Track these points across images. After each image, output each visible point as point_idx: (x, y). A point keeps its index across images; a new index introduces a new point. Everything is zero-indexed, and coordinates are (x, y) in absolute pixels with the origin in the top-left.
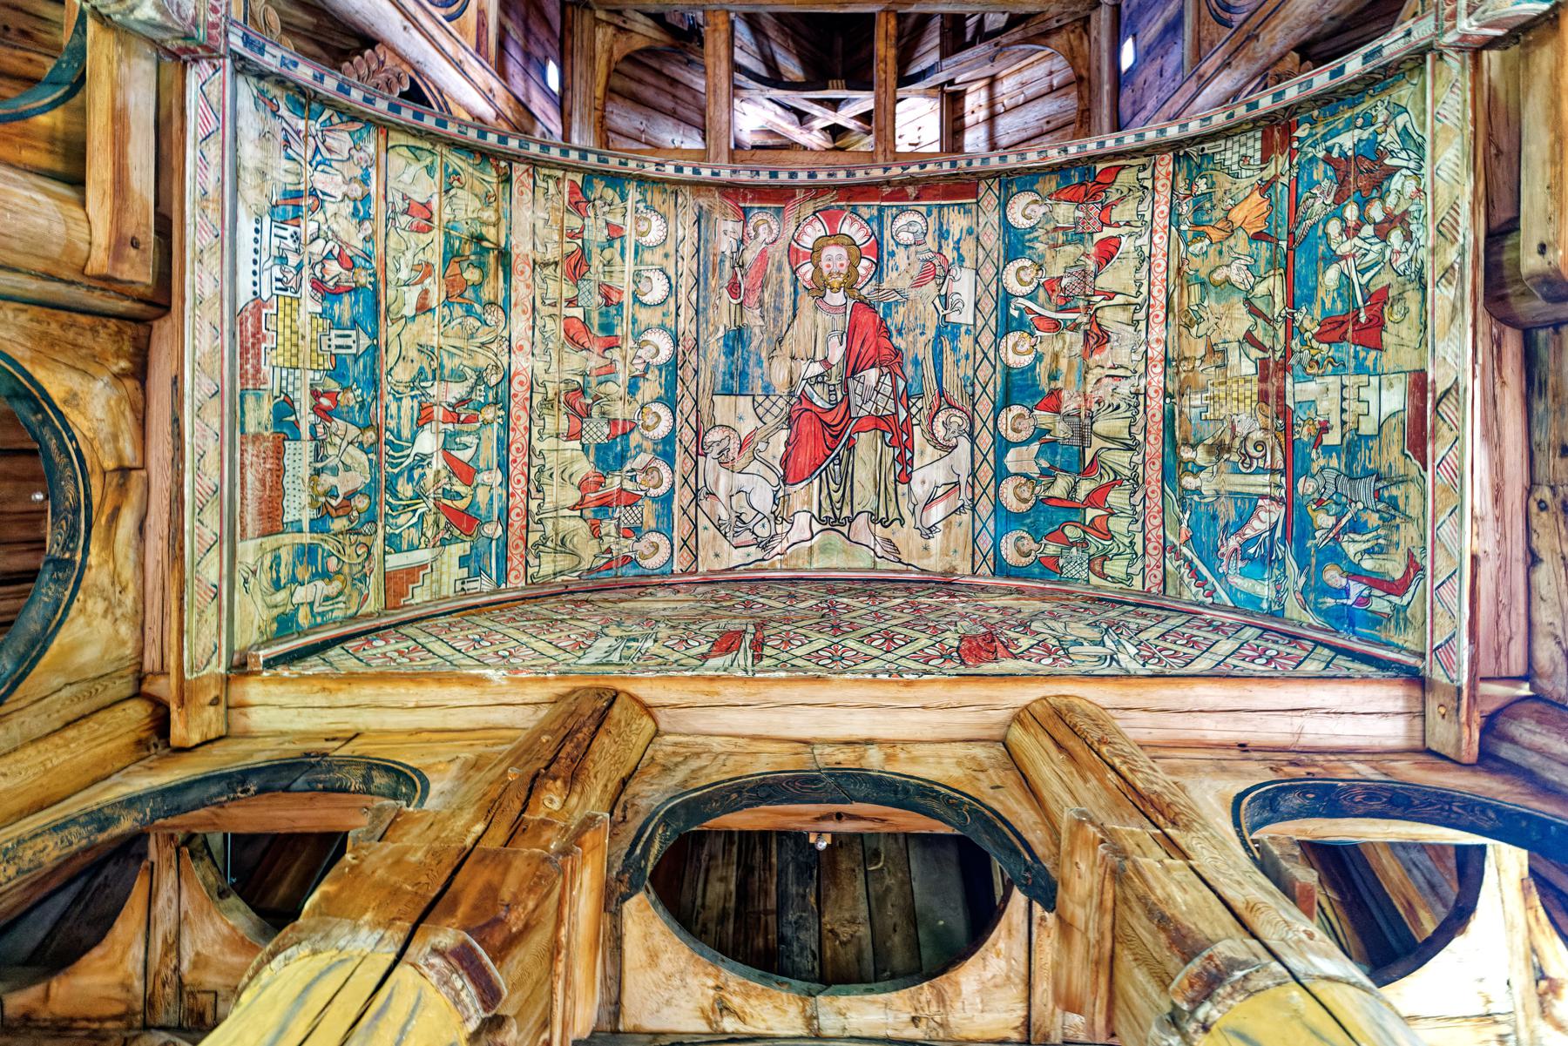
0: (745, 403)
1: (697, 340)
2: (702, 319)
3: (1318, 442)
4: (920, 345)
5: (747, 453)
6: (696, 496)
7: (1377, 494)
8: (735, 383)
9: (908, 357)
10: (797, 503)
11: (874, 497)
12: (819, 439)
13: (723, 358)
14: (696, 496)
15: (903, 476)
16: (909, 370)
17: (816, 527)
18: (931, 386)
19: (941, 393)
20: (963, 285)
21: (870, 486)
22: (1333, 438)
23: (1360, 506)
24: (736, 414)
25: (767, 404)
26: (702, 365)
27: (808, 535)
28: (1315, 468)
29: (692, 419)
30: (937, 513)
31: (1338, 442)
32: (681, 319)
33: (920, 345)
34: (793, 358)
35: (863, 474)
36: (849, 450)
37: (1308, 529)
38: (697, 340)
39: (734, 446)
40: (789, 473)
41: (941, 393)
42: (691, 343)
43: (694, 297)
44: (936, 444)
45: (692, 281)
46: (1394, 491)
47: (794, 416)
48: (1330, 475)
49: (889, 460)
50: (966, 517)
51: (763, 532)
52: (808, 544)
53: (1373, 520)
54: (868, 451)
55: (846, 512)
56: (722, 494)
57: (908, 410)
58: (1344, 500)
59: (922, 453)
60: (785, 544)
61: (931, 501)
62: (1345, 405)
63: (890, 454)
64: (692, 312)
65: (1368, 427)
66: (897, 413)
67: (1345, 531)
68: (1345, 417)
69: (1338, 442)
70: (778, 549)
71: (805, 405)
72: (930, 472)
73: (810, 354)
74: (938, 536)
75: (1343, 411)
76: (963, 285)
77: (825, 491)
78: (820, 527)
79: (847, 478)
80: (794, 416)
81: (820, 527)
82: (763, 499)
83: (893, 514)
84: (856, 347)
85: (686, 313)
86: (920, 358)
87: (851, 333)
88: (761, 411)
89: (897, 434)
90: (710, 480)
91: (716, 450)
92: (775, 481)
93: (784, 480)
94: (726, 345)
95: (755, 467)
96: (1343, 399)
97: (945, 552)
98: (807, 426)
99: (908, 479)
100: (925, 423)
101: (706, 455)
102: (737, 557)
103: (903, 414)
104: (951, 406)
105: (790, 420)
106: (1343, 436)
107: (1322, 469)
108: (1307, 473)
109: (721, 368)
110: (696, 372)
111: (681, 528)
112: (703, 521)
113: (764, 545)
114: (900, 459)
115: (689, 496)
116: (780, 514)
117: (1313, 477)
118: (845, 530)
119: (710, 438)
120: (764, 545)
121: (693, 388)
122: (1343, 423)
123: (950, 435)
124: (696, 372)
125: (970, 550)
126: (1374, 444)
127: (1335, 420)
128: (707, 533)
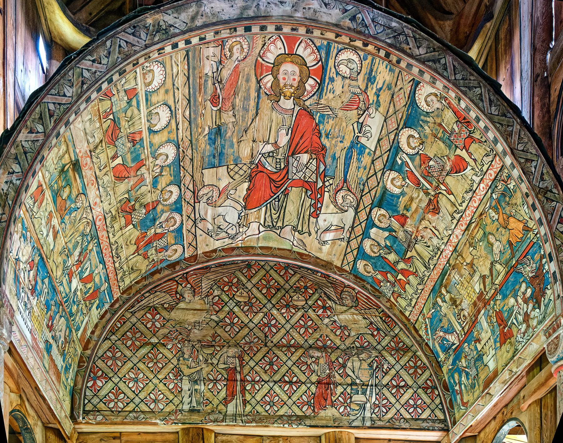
0: (222, 171)
1: (191, 141)
2: (193, 125)
4: (338, 149)
5: (223, 196)
6: (195, 222)
8: (217, 159)
9: (329, 154)
10: (252, 218)
11: (296, 220)
12: (267, 186)
13: (208, 147)
14: (195, 222)
15: (314, 214)
16: (329, 160)
17: (262, 229)
18: (340, 174)
19: (345, 181)
20: (374, 122)
21: (295, 214)
24: (219, 177)
25: (236, 169)
26: (195, 155)
27: (258, 232)
29: (191, 187)
30: (329, 236)
32: (180, 131)
33: (338, 149)
34: (254, 141)
35: (292, 208)
36: (285, 195)
38: (191, 141)
39: (216, 194)
40: (249, 203)
41: (345, 181)
42: (187, 143)
43: (187, 113)
44: (336, 205)
45: (185, 103)
47: (253, 175)
49: (308, 204)
50: (344, 244)
51: (232, 232)
52: (257, 236)
54: (295, 199)
55: (280, 224)
56: (209, 218)
57: (324, 182)
59: (327, 207)
60: (244, 236)
61: (327, 230)
63: (308, 202)
64: (187, 124)
66: (317, 182)
70: (241, 238)
71: (260, 168)
72: (329, 217)
73: (266, 139)
74: (328, 246)
76: (374, 122)
77: (268, 213)
78: (264, 229)
79: (282, 209)
80: (253, 175)
81: (264, 229)
82: (232, 216)
83: (305, 229)
84: (297, 139)
85: (183, 125)
86: (337, 156)
87: (294, 130)
88: (232, 173)
89: (314, 192)
90: (202, 213)
91: (205, 198)
92: (239, 208)
93: (245, 208)
94: (210, 139)
95: (228, 202)
97: (329, 254)
98: (262, 181)
99: (317, 216)
100: (332, 193)
101: (199, 202)
102: (218, 244)
103: (320, 184)
104: (349, 190)
105: (251, 178)
109: (207, 153)
110: (192, 160)
111: (187, 238)
112: (199, 232)
113: (233, 238)
114: (314, 205)
115: (191, 223)
116: (243, 222)
118: (278, 232)
119: (201, 193)
120: (233, 238)
121: (190, 170)
123: (344, 204)
124: (192, 160)
125: (342, 257)
128: (201, 236)
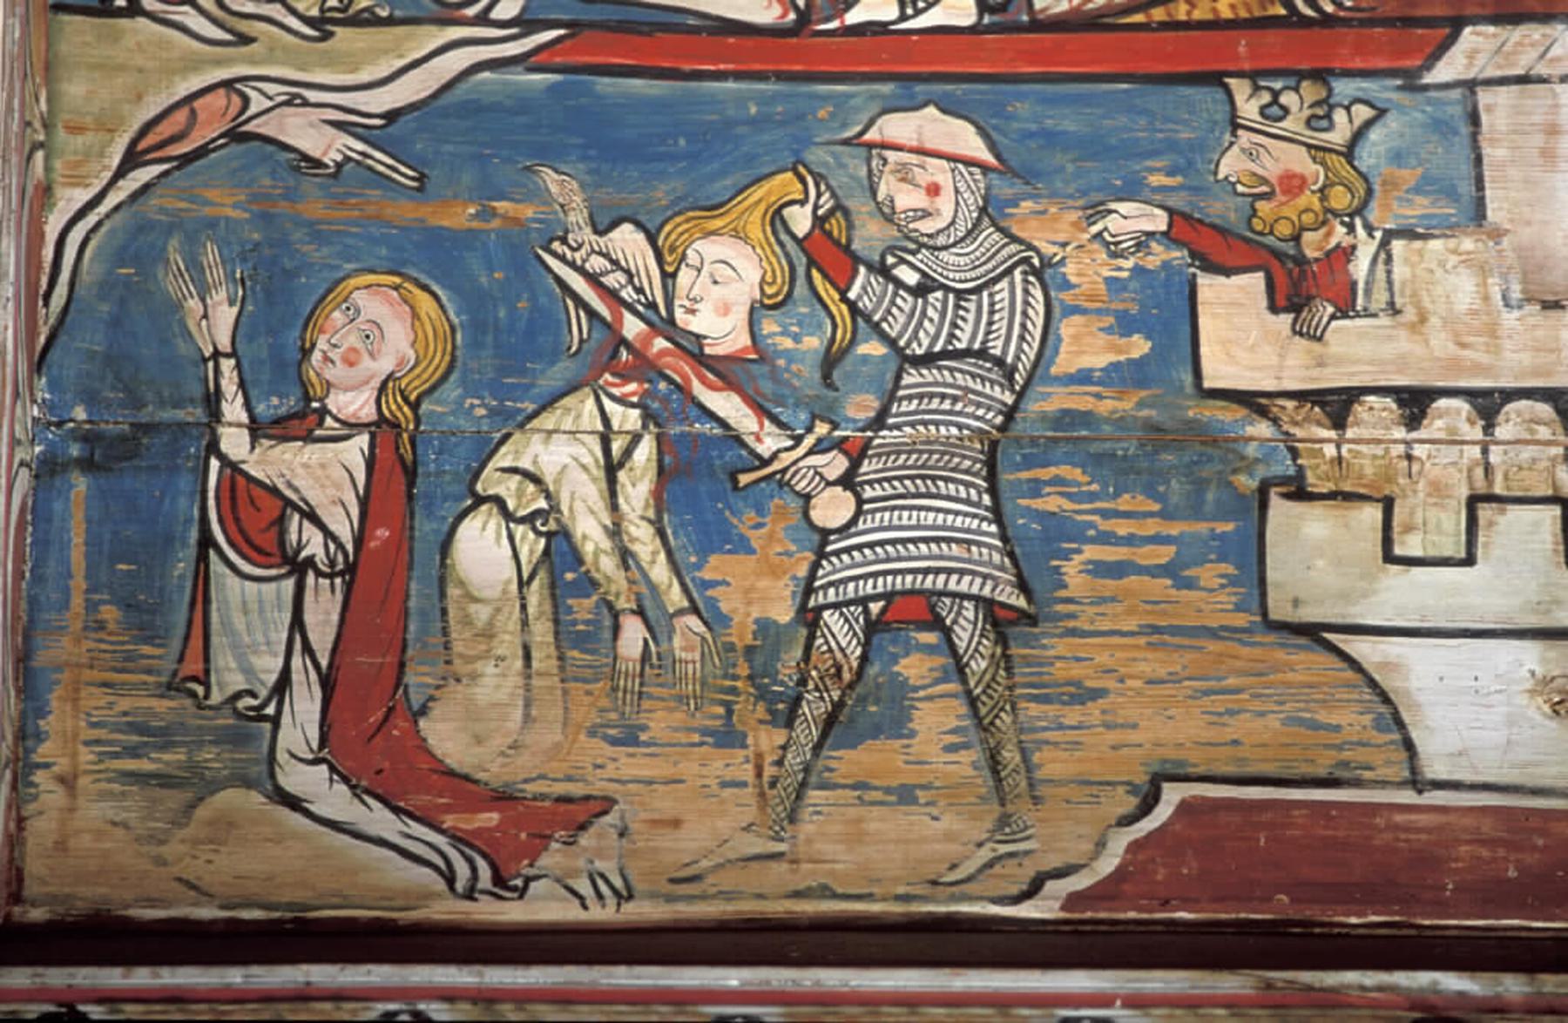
3: (1209, 242)
7: (905, 614)
22: (1240, 336)
23: (832, 509)
28: (1048, 228)
31: (1218, 373)
37: (673, 179)
46: (936, 719)
48: (1008, 319)
53: (758, 593)
58: (861, 406)
62: (1451, 415)
65: (1313, 552)
67: (666, 410)
68: (1375, 415)
69: (1218, 373)
75: (1415, 403)
96: (1488, 404)
106: (1253, 402)
107: (1042, 271)
108: (1012, 171)
117: (990, 212)
122: (1337, 405)
126: (1213, 595)
127: (1357, 350)
